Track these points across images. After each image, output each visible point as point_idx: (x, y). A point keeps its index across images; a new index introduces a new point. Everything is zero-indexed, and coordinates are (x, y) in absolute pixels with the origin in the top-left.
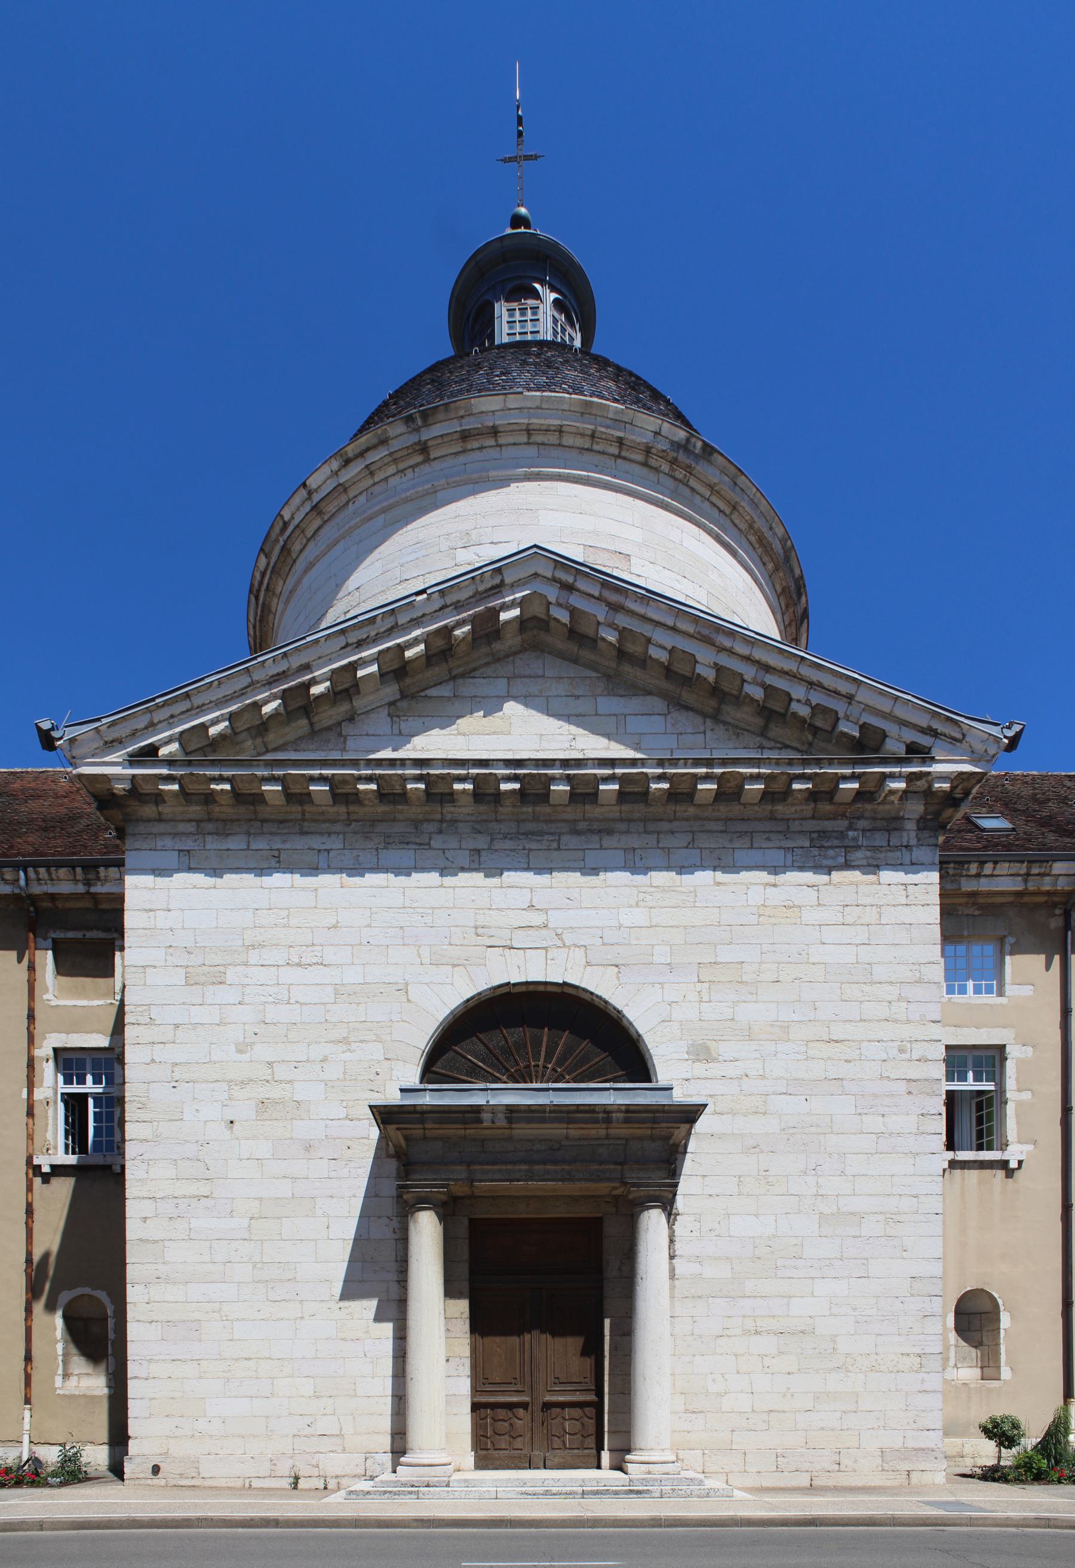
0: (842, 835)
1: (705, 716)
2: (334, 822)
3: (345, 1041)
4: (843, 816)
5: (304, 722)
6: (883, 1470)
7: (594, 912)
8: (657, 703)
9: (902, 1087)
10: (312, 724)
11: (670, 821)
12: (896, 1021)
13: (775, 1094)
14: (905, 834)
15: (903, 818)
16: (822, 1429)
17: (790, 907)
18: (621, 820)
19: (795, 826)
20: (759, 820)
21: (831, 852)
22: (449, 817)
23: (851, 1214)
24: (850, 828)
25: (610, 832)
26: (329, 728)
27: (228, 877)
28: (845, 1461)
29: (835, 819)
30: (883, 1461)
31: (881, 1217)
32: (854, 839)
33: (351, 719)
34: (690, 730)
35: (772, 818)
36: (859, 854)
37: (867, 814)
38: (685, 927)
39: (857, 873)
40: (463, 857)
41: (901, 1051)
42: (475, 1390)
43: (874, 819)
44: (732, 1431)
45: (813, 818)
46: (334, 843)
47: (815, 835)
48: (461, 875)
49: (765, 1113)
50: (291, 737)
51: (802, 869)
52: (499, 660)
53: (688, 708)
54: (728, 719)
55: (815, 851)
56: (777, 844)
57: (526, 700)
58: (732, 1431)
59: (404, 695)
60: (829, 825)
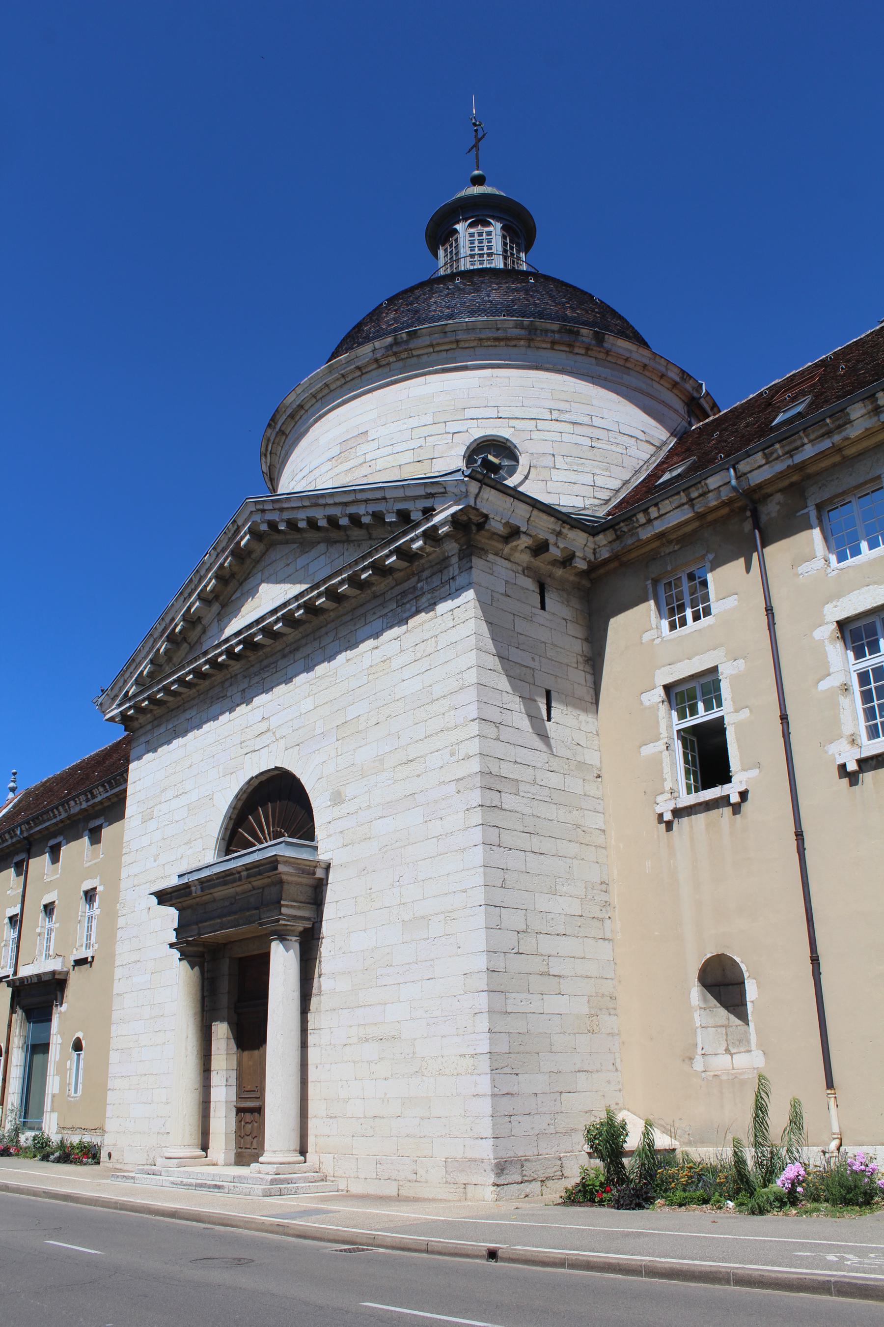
0: (414, 588)
1: (343, 542)
2: (193, 699)
3: (189, 842)
4: (413, 574)
5: (185, 645)
6: (446, 1182)
7: (288, 710)
8: (322, 547)
9: (452, 787)
10: (189, 644)
11: (326, 626)
12: (448, 729)
13: (376, 819)
14: (451, 568)
15: (449, 557)
16: (408, 1136)
17: (385, 661)
18: (303, 638)
19: (388, 596)
20: (369, 601)
21: (408, 606)
22: (233, 674)
23: (422, 917)
24: (419, 581)
25: (297, 649)
26: (197, 642)
27: (160, 750)
28: (421, 1171)
29: (409, 579)
30: (446, 1172)
31: (441, 917)
32: (422, 588)
33: (204, 632)
34: (337, 556)
35: (375, 597)
36: (424, 599)
37: (426, 566)
38: (331, 701)
39: (423, 614)
40: (237, 698)
41: (452, 755)
42: (239, 1098)
43: (432, 567)
44: (353, 1136)
45: (397, 585)
46: (193, 712)
47: (399, 597)
48: (238, 709)
49: (370, 838)
50: (183, 655)
51: (391, 627)
52: (258, 562)
53: (336, 542)
54: (354, 538)
55: (399, 610)
56: (379, 614)
57: (268, 580)
58: (353, 1136)
59: (223, 606)
60: (406, 585)
